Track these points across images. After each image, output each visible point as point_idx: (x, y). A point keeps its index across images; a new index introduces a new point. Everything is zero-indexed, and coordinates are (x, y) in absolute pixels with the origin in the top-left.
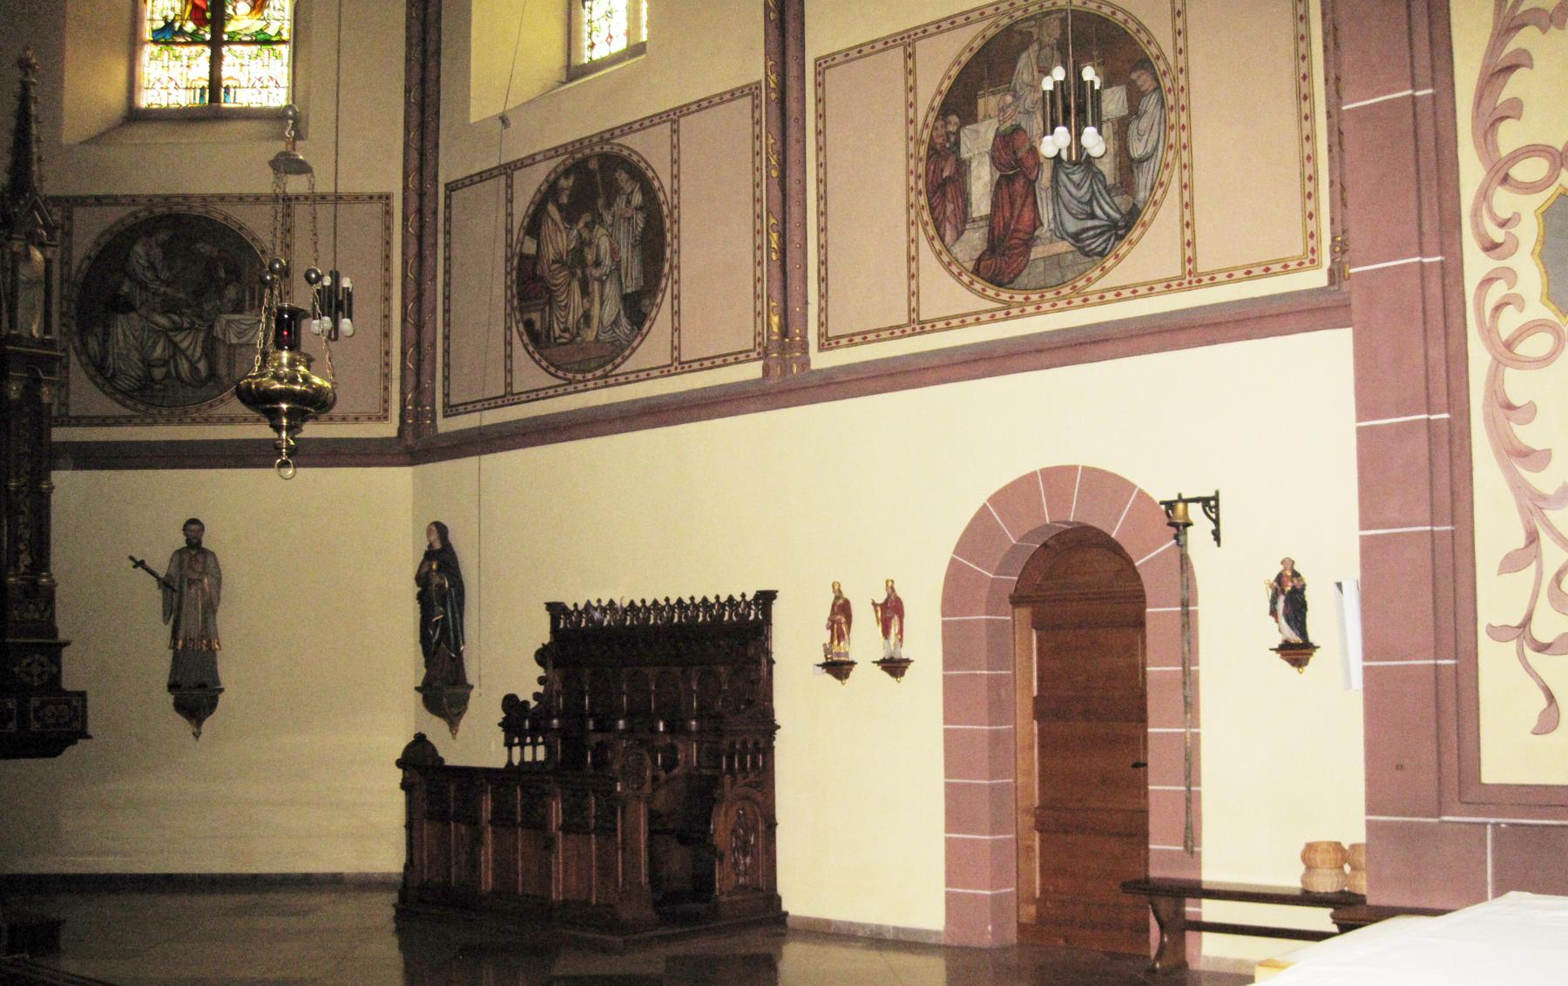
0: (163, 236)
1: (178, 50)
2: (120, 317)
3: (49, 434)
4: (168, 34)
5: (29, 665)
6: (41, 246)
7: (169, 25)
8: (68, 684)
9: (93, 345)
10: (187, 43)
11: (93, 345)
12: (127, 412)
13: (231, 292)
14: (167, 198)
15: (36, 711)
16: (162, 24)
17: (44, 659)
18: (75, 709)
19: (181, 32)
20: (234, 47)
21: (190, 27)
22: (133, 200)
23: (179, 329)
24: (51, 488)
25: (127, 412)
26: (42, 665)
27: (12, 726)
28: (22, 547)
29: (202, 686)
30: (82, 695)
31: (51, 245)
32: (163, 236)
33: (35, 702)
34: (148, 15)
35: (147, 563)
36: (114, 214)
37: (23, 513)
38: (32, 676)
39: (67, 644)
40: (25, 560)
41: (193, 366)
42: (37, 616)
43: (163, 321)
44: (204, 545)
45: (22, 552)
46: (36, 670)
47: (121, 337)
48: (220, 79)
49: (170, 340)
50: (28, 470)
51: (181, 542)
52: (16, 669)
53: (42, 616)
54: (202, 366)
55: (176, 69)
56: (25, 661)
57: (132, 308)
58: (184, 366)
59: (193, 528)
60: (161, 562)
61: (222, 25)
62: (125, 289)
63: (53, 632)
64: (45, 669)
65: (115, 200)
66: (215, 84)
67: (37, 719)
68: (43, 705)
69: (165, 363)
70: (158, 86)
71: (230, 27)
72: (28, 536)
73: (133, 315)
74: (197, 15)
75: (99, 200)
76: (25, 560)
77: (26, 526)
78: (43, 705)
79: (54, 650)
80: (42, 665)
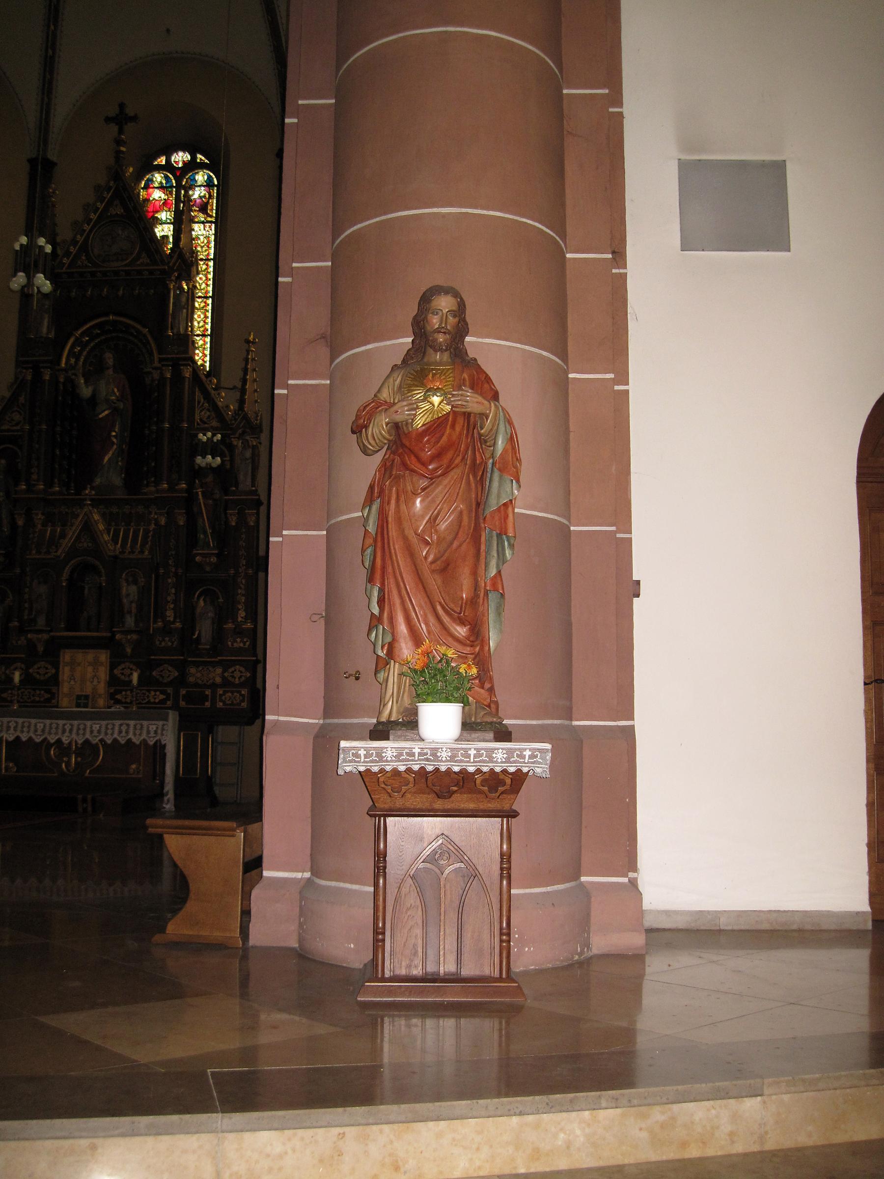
5: (233, 672)
15: (221, 695)
17: (242, 669)
26: (241, 672)
27: (208, 704)
28: (240, 607)
33: (220, 691)
37: (241, 588)
38: (235, 678)
42: (242, 645)
45: (240, 610)
46: (237, 674)
50: (244, 563)
53: (244, 645)
56: (231, 670)
64: (244, 674)
67: (221, 700)
72: (243, 601)
77: (243, 595)
78: (225, 692)
80: (241, 672)
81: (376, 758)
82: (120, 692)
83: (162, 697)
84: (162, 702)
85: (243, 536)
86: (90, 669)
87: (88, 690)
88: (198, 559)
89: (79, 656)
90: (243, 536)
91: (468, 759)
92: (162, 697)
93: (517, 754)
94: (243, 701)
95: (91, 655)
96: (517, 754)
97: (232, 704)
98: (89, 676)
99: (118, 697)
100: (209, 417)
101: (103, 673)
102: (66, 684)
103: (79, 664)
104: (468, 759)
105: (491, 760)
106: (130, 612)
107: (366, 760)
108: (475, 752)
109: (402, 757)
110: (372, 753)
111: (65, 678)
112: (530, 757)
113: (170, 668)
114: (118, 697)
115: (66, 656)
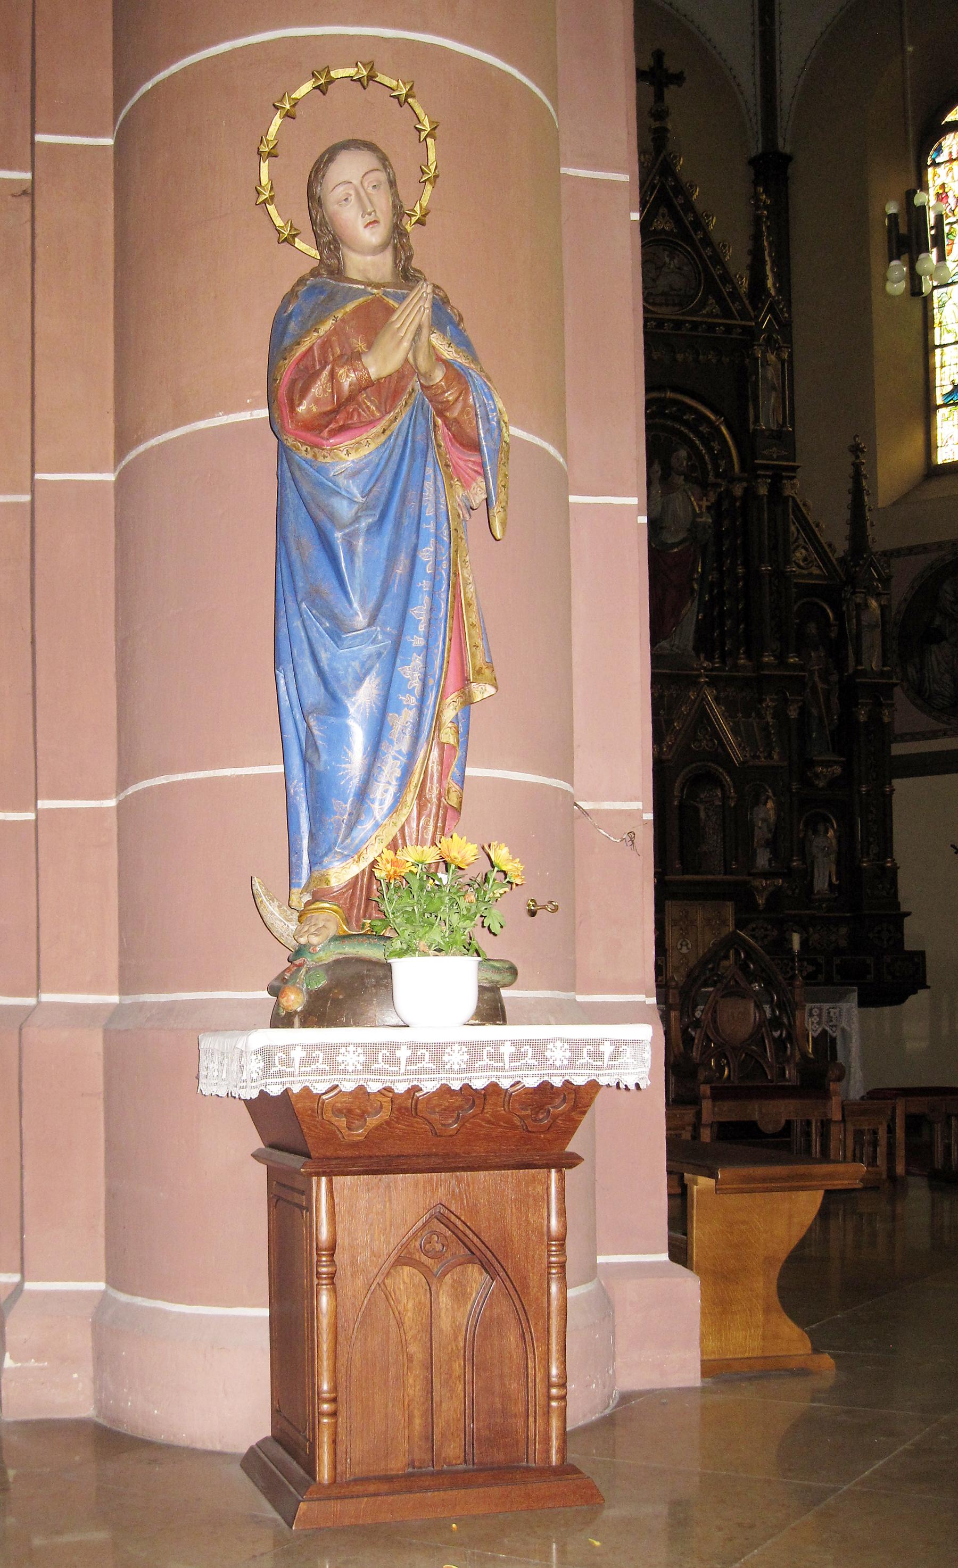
2: (934, 648)
3: (889, 748)
6: (878, 595)
8: (910, 945)
9: (911, 671)
11: (911, 671)
12: (942, 726)
16: (949, 388)
22: (940, 546)
24: (892, 791)
25: (942, 726)
27: (870, 977)
30: (922, 954)
31: (885, 594)
34: (938, 383)
37: (871, 812)
39: (908, 914)
40: (874, 849)
47: (935, 663)
52: (871, 935)
62: (937, 622)
63: (898, 905)
65: (925, 549)
70: (950, 442)
73: (944, 643)
75: (911, 550)
79: (897, 919)
81: (324, 1066)
83: (811, 969)
91: (397, 1069)
92: (811, 969)
93: (489, 1053)
96: (489, 1053)
100: (805, 559)
104: (397, 1069)
105: (334, 1068)
107: (409, 1068)
108: (304, 1054)
109: (376, 1066)
110: (423, 1055)
112: (410, 1061)
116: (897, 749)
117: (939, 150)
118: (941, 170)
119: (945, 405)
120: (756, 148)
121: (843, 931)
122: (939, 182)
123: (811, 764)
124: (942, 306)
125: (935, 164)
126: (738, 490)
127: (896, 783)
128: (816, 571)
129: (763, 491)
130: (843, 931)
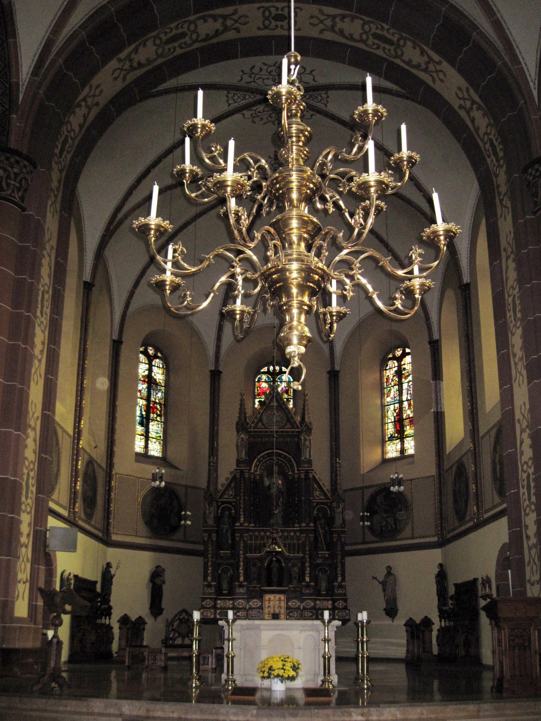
0: (384, 494)
1: (394, 442)
4: (392, 438)
7: (391, 435)
10: (396, 440)
13: (400, 506)
14: (384, 484)
16: (390, 436)
18: (347, 613)
19: (394, 437)
20: (407, 439)
21: (396, 435)
22: (377, 485)
23: (388, 517)
29: (392, 609)
32: (384, 494)
35: (378, 578)
36: (372, 490)
40: (340, 579)
41: (391, 526)
43: (385, 516)
44: (392, 572)
46: (340, 604)
48: (404, 448)
49: (386, 520)
51: (386, 572)
54: (394, 526)
55: (394, 446)
57: (378, 513)
58: (390, 527)
59: (389, 568)
60: (381, 579)
61: (404, 433)
66: (403, 450)
68: (339, 612)
69: (385, 526)
71: (406, 433)
74: (398, 431)
76: (340, 579)
78: (339, 612)
82: (292, 612)
83: (311, 614)
84: (311, 616)
85: (339, 546)
86: (278, 602)
87: (277, 612)
88: (319, 555)
89: (272, 596)
90: (339, 546)
92: (311, 614)
94: (347, 615)
95: (278, 596)
97: (342, 617)
98: (277, 606)
99: (291, 614)
101: (283, 604)
102: (266, 609)
103: (272, 601)
106: (295, 578)
111: (266, 606)
113: (310, 602)
114: (291, 614)
115: (267, 597)
116: (347, 548)
117: (387, 365)
118: (388, 371)
119: (389, 441)
120: (329, 369)
121: (330, 602)
122: (387, 375)
123: (318, 554)
124: (388, 411)
125: (386, 370)
126: (296, 476)
127: (346, 558)
128: (323, 497)
129: (303, 476)
130: (330, 602)
